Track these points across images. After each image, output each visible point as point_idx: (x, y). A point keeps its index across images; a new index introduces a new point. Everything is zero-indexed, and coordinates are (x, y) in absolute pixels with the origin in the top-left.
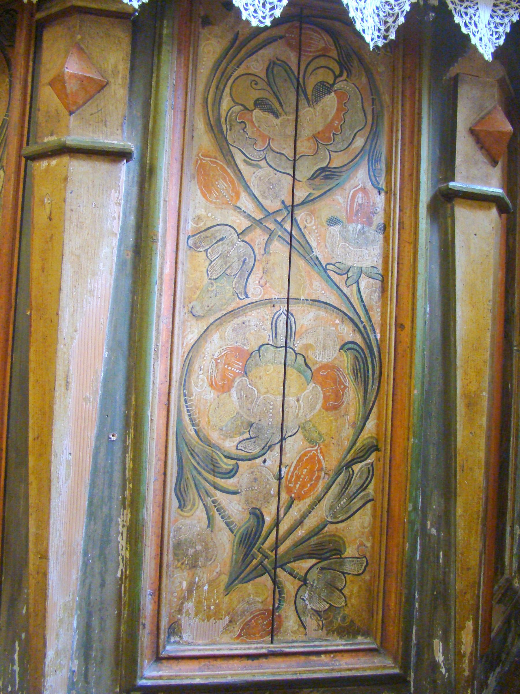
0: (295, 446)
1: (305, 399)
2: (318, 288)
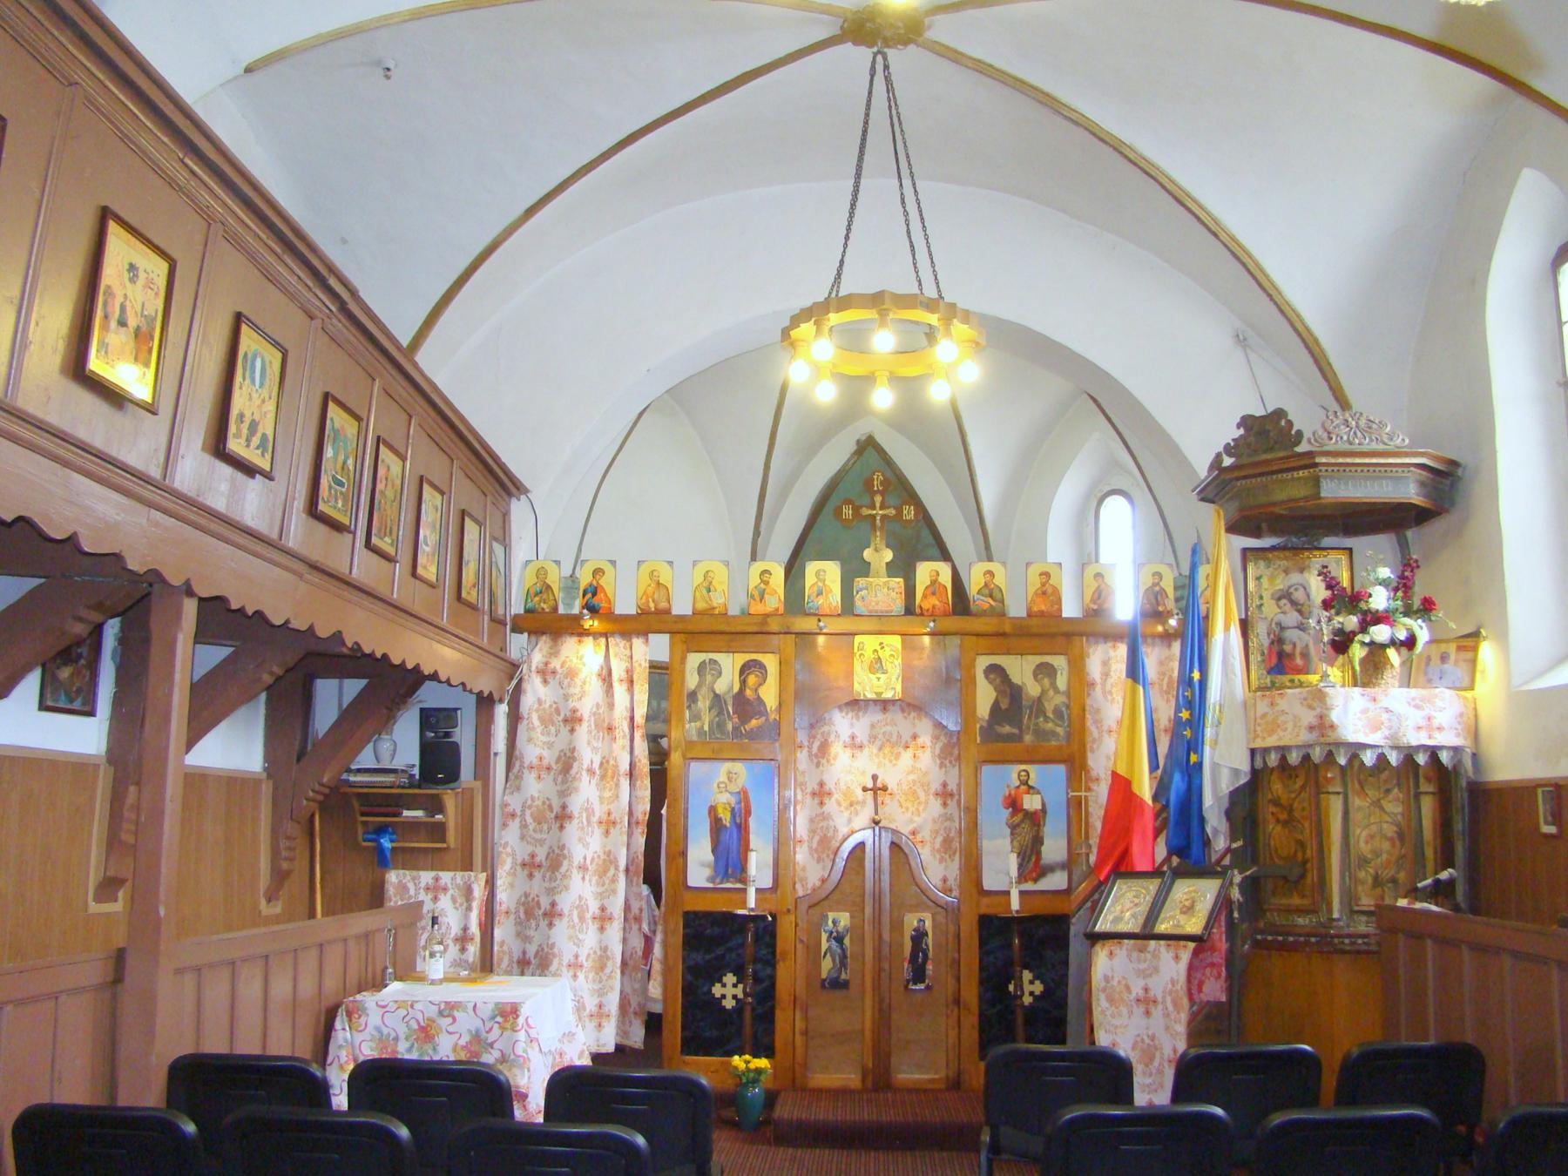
0: (1385, 856)
1: (1386, 846)
2: (1387, 818)
